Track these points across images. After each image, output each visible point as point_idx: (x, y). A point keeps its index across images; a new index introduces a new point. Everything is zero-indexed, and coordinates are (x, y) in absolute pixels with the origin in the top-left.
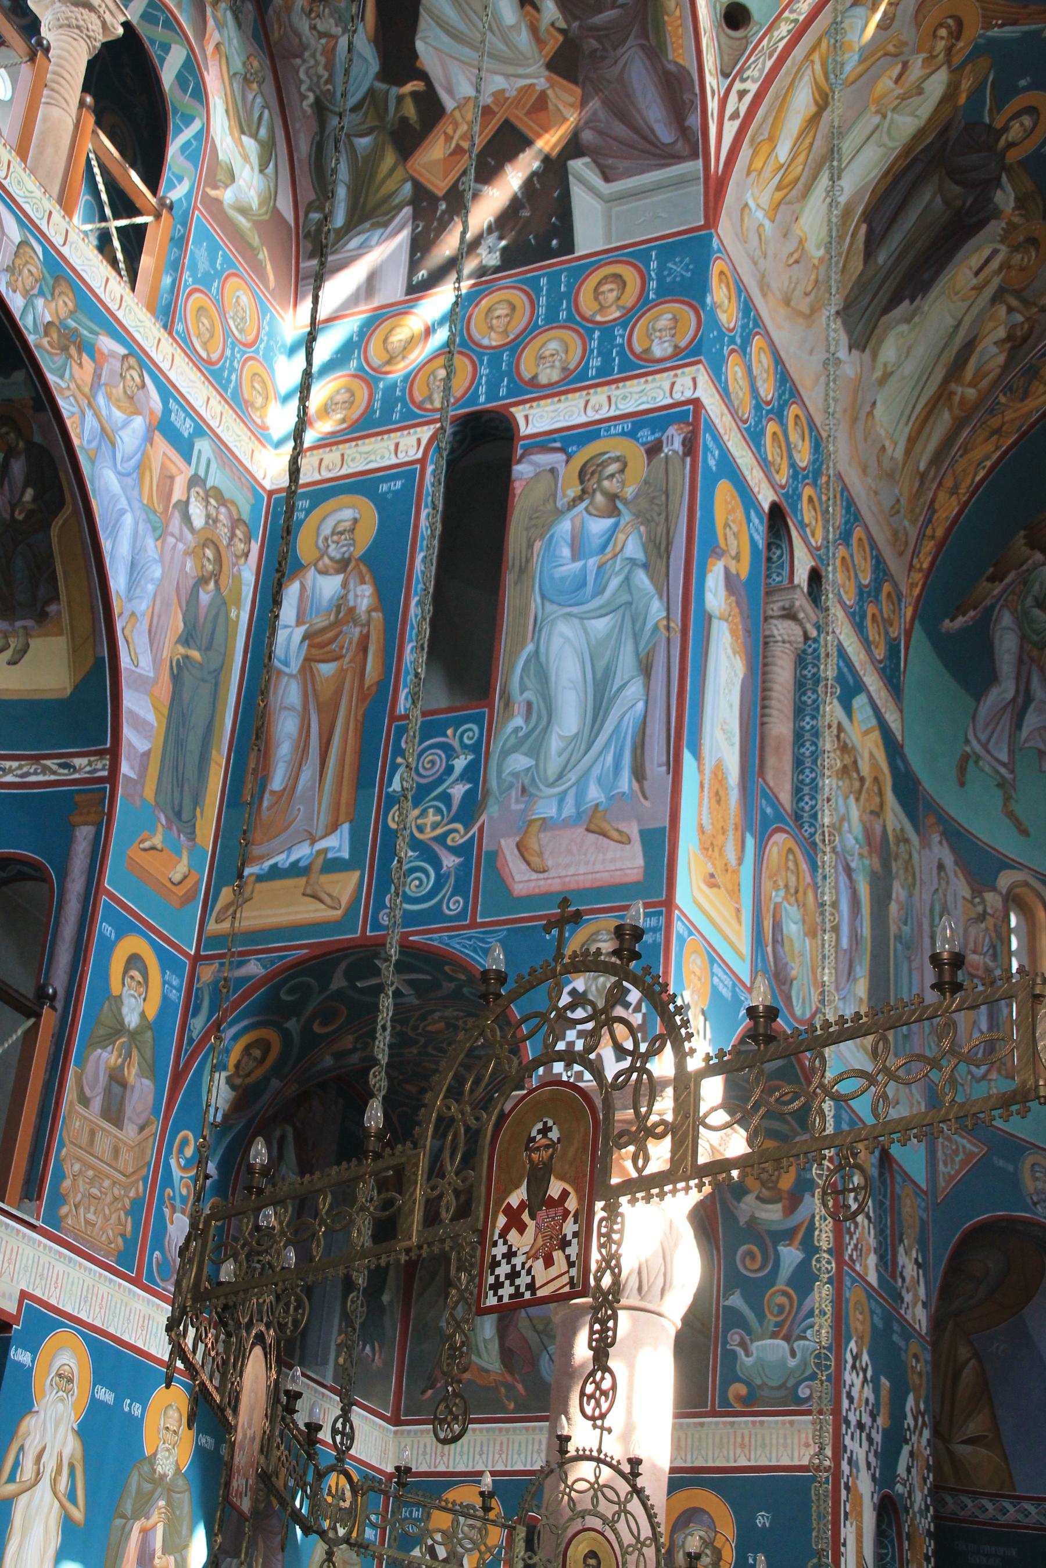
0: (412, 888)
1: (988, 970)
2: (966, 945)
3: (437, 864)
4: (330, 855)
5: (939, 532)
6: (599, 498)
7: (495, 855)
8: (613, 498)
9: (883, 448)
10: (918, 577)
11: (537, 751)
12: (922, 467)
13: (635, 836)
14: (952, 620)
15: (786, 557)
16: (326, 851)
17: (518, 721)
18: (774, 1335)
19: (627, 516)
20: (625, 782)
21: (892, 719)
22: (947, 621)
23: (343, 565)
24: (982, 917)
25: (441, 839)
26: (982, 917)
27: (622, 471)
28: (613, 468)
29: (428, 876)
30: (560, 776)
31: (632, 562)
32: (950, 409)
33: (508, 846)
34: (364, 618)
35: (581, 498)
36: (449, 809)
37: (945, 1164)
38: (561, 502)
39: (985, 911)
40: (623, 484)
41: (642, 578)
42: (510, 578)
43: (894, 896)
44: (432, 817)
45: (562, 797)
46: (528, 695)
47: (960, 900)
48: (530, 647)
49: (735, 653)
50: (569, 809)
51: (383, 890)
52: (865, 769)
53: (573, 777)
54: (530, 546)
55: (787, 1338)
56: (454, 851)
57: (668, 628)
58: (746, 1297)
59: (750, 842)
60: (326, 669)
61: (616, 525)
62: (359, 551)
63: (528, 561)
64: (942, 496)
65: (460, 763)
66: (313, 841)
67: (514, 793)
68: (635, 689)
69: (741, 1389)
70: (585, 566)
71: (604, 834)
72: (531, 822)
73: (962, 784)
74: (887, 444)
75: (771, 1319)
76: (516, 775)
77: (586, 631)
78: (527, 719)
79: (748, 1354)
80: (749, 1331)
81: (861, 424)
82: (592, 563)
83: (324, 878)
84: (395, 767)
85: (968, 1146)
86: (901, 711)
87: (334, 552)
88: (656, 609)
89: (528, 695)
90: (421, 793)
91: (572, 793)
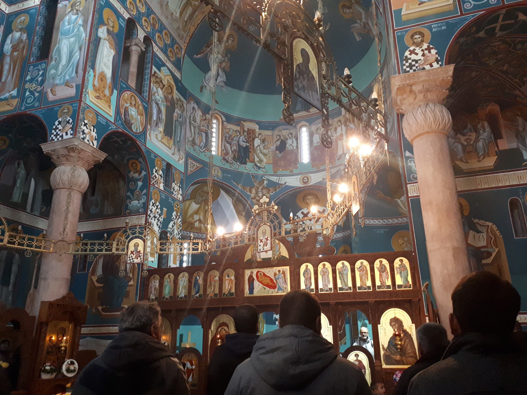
0: (28, 101)
1: (206, 130)
2: (200, 125)
3: (34, 95)
4: (13, 95)
5: (191, 35)
6: (75, 11)
7: (46, 92)
8: (77, 10)
9: (173, 13)
10: (186, 45)
11: (56, 68)
12: (186, 19)
13: (74, 86)
14: (197, 55)
15: (136, 32)
16: (12, 94)
17: (53, 62)
18: (136, 200)
19: (80, 14)
20: (74, 74)
21: (178, 75)
22: (195, 55)
23: (21, 30)
24: (205, 119)
25: (35, 90)
26: (205, 119)
27: (80, 4)
28: (78, 4)
29: (32, 98)
30: (61, 74)
31: (80, 24)
32: (192, 6)
33: (49, 90)
34: (24, 41)
35: (71, 11)
36: (38, 83)
37: (191, 168)
38: (67, 12)
39: (206, 118)
40: (80, 7)
41: (82, 29)
42: (55, 30)
43: (176, 112)
44: (34, 85)
45: (61, 79)
46: (56, 56)
47: (199, 115)
48: (57, 46)
49: (111, 48)
50: (62, 81)
51: (23, 102)
52: (165, 82)
53: (63, 74)
54: (60, 22)
55: (138, 201)
56: (38, 92)
57: (86, 39)
58: (131, 193)
59: (115, 92)
60: (16, 54)
61: (77, 17)
62: (24, 27)
63: (59, 26)
64: (192, 27)
65: (41, 73)
66: (9, 92)
67: (51, 78)
68: (77, 54)
69: (129, 211)
70: (70, 27)
71: (68, 86)
72: (54, 85)
73: (201, 92)
74: (174, 13)
75: (135, 197)
76: (52, 74)
77: (69, 41)
78: (55, 61)
79: (130, 204)
80: (130, 199)
81: (164, 7)
82: (72, 25)
83: (11, 100)
84: (28, 75)
85: (198, 165)
86: (181, 74)
87: (19, 27)
88: (84, 35)
89: (56, 56)
90: (31, 81)
91: (63, 77)
